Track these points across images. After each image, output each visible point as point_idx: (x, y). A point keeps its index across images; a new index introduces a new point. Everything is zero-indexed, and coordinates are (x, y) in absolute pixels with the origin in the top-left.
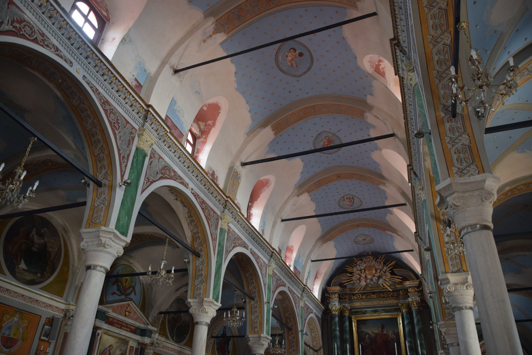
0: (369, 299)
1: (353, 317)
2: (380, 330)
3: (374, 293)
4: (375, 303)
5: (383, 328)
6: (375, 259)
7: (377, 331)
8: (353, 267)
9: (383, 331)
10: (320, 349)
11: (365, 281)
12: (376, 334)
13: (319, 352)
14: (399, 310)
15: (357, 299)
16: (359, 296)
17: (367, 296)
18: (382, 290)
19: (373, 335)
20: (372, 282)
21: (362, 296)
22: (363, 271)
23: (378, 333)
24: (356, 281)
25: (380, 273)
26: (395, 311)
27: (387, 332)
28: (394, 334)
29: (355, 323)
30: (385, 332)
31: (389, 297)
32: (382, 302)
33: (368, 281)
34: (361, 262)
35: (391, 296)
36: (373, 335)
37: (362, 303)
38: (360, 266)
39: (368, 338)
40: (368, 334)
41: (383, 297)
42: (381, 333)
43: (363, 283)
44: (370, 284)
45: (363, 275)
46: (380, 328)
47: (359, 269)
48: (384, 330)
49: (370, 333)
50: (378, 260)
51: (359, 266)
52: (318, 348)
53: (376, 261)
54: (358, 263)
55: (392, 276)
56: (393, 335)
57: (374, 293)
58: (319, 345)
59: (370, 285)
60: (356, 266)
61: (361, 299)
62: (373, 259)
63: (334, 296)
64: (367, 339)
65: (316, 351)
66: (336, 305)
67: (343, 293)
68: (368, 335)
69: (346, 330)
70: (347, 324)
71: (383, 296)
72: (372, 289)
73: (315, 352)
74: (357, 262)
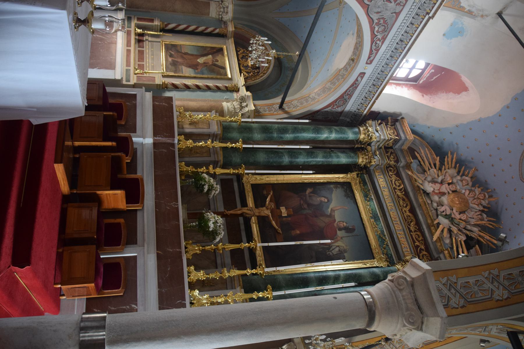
0: (399, 202)
1: (354, 174)
2: (342, 225)
3: (412, 211)
4: (393, 213)
5: (347, 230)
6: (486, 210)
7: (338, 216)
8: (455, 168)
9: (340, 229)
10: (286, 112)
11: (433, 191)
12: (331, 216)
13: (280, 112)
14: (390, 263)
15: (391, 181)
16: (398, 184)
17: (403, 200)
18: (424, 227)
19: (329, 210)
20: (435, 205)
21: (400, 190)
22: (452, 188)
23: (335, 221)
24: (430, 175)
25: (460, 219)
26: (387, 254)
27: (341, 238)
28: (339, 250)
29: (342, 178)
30: (340, 233)
31: (414, 242)
32: (398, 228)
33: (436, 198)
34: (470, 184)
35: (417, 247)
36: (329, 210)
37: (386, 190)
38: (460, 183)
39: (321, 201)
40: (328, 201)
41: (409, 229)
42: (335, 225)
43: (429, 188)
44: (432, 201)
45: (444, 188)
46: (345, 224)
47: (455, 181)
48: (343, 231)
49: (332, 205)
50: (485, 216)
51: (462, 181)
52: (287, 109)
53: (483, 211)
54: (467, 178)
55: (463, 243)
56: (337, 249)
57: (412, 211)
58: (294, 109)
59: (429, 202)
60: (458, 173)
61: (395, 189)
62: (484, 207)
63: (392, 131)
64: (318, 199)
65: (281, 106)
66: (376, 132)
67: (399, 153)
68: (326, 200)
69: (331, 157)
70: (343, 159)
71: (412, 229)
72: (423, 205)
73: (278, 105)
74: (467, 176)
